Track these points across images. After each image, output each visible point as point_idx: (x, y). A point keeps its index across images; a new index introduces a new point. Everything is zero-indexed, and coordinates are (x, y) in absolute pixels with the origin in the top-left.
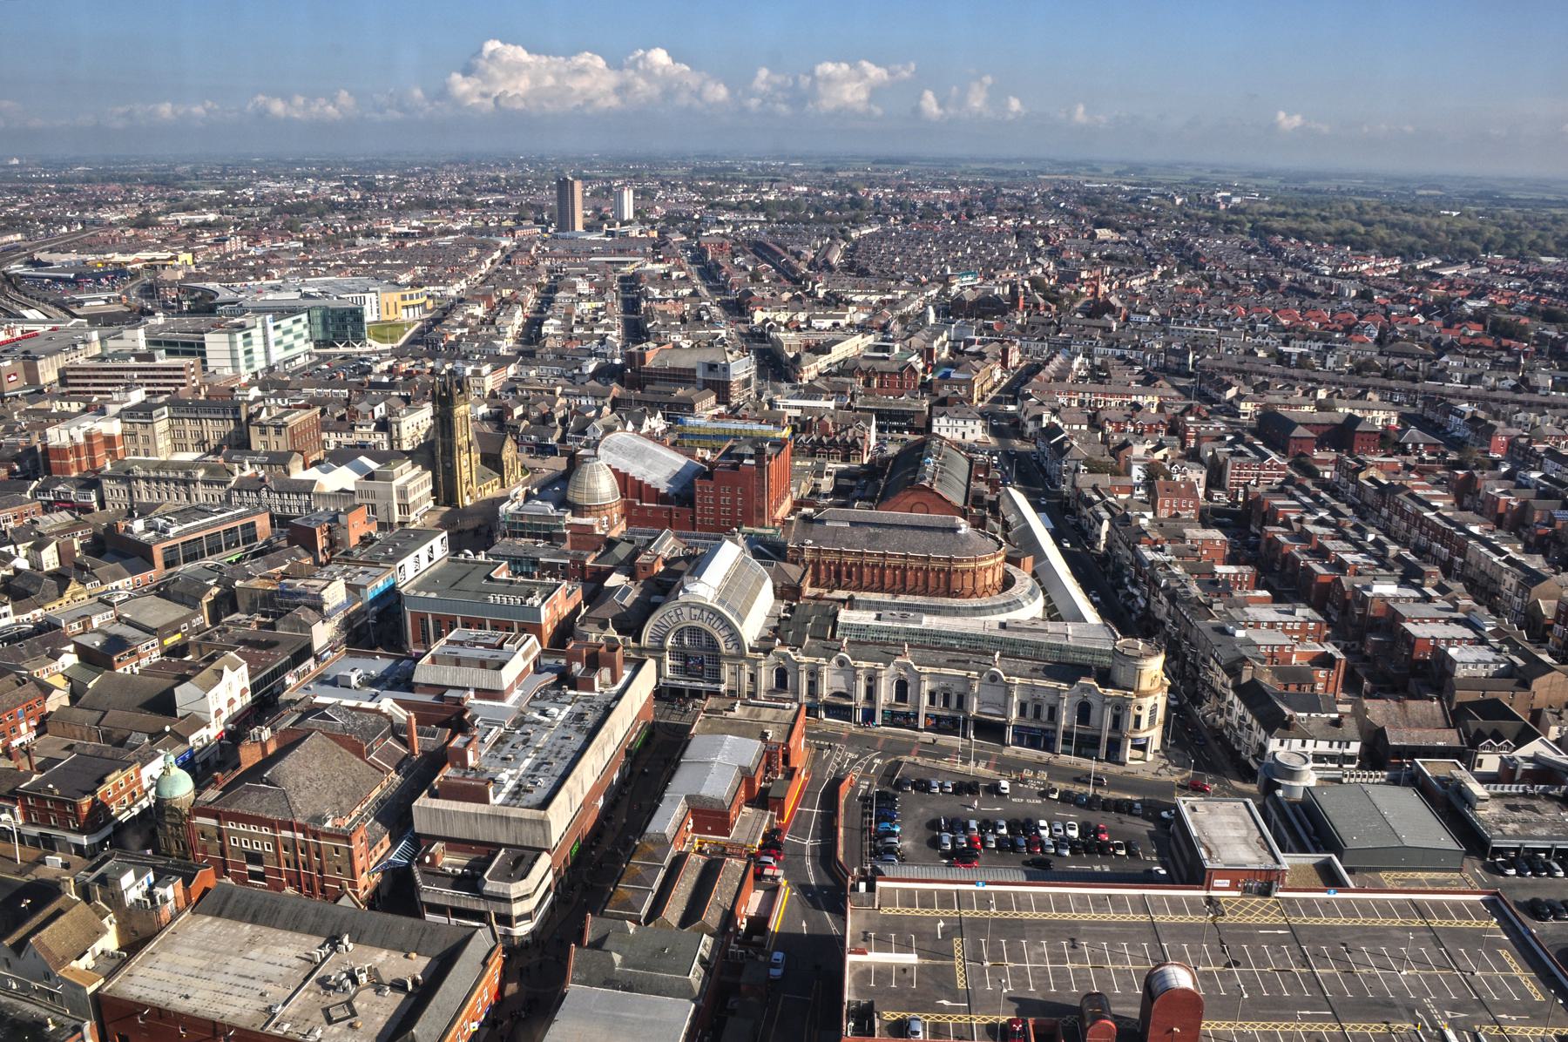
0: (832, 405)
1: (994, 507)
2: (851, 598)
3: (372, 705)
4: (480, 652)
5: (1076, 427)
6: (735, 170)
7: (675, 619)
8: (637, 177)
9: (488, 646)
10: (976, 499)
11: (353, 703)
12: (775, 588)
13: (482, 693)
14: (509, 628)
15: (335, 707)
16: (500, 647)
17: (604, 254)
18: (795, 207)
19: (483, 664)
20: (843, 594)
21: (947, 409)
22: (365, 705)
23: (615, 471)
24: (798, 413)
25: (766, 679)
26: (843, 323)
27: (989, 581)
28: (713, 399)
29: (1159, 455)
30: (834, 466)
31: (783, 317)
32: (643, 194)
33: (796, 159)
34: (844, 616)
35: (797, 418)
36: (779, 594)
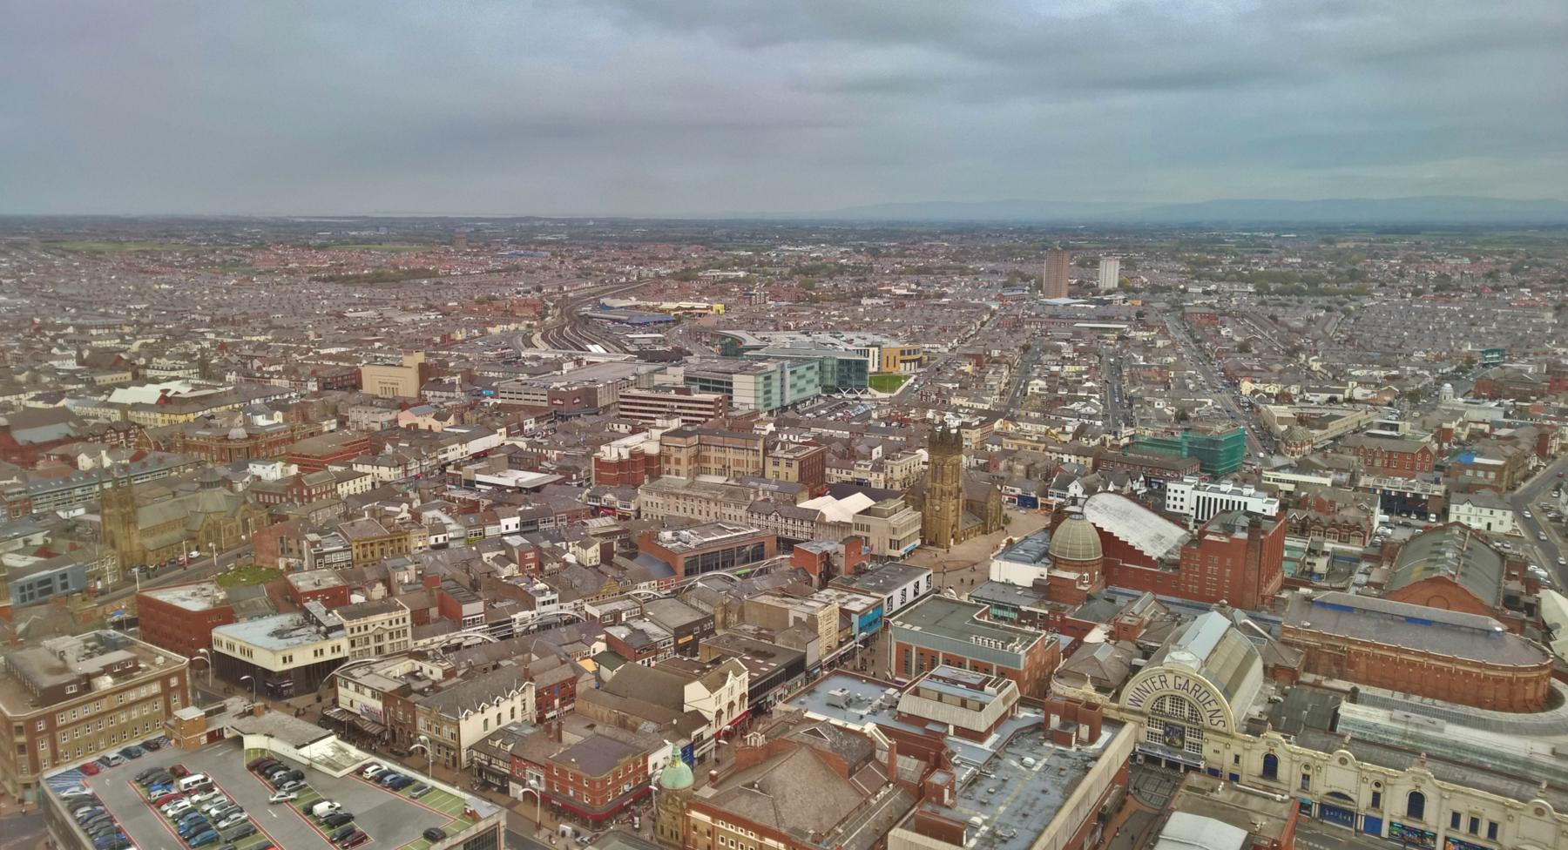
0: (1328, 482)
1: (1532, 609)
2: (1355, 691)
3: (857, 728)
4: (961, 691)
6: (1222, 242)
7: (1158, 685)
8: (1124, 248)
9: (970, 686)
10: (1511, 601)
11: (840, 723)
12: (1265, 668)
13: (962, 732)
14: (987, 670)
15: (825, 724)
16: (982, 689)
17: (1088, 320)
18: (1285, 278)
19: (964, 704)
20: (1345, 685)
21: (1471, 496)
22: (851, 726)
23: (1100, 530)
24: (1291, 487)
25: (1254, 763)
26: (1340, 397)
27: (1530, 695)
28: (1197, 468)
31: (1274, 389)
32: (1129, 264)
33: (1288, 230)
34: (1347, 710)
35: (1288, 493)
36: (1271, 673)
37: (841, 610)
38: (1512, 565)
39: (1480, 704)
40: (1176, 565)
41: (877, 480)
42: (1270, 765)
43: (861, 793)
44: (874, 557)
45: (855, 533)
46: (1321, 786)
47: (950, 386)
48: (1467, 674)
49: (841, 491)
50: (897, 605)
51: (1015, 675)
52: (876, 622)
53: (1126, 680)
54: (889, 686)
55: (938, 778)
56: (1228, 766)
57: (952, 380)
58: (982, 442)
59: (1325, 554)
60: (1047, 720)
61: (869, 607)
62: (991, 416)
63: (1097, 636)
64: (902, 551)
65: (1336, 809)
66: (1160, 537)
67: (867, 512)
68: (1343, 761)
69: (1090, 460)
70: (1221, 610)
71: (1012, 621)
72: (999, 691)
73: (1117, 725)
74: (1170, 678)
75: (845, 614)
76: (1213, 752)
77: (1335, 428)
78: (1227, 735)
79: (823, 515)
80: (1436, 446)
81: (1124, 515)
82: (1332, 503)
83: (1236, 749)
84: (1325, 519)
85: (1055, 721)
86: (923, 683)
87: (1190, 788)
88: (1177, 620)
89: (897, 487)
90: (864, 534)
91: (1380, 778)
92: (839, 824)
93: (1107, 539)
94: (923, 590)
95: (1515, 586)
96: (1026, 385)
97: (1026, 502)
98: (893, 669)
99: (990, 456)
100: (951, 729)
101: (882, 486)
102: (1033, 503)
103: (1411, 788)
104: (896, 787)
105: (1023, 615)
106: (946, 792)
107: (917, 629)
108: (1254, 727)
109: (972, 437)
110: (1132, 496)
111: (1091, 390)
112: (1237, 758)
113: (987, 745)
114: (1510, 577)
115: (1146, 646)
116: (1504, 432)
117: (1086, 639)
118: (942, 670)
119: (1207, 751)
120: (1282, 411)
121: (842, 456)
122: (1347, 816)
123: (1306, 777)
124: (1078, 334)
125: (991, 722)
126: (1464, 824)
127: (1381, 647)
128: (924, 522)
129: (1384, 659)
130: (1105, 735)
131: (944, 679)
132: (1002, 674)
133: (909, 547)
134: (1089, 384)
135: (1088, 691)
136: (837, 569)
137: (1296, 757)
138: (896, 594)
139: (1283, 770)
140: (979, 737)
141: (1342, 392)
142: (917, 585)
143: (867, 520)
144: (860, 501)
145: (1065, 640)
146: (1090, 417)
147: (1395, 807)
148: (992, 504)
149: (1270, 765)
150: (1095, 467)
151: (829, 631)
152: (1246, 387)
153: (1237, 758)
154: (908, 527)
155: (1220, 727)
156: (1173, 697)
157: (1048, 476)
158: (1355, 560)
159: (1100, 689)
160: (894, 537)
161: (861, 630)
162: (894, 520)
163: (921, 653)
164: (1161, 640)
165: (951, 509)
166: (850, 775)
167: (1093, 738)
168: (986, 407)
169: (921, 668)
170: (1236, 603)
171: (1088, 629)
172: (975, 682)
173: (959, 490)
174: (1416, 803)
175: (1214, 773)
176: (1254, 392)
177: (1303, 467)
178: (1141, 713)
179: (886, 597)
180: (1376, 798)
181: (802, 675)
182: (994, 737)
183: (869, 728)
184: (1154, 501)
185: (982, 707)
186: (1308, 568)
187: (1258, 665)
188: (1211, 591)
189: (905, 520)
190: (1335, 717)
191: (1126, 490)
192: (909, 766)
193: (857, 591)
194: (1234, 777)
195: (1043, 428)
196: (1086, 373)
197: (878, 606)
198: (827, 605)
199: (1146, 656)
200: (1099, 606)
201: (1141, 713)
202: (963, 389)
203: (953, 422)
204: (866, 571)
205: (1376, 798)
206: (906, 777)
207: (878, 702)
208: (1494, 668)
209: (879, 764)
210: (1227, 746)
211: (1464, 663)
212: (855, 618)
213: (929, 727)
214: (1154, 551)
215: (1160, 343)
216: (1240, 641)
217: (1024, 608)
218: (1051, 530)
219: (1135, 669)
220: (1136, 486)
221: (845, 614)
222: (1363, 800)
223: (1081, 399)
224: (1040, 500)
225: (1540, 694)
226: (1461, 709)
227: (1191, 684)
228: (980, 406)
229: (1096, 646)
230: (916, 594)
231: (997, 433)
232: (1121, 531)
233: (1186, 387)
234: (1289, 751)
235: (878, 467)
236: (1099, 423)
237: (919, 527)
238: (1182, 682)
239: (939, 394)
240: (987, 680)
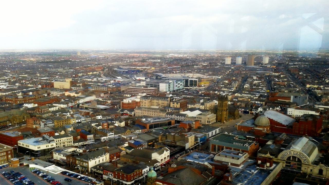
3: (202, 163)
13: (232, 164)
16: (238, 155)
19: (233, 158)
36: (320, 151)
44: (203, 125)
45: (197, 119)
47: (222, 86)
50: (210, 136)
51: (247, 151)
54: (211, 154)
55: (227, 174)
57: (222, 84)
58: (232, 99)
61: (202, 136)
62: (234, 93)
70: (306, 136)
71: (244, 139)
72: (243, 155)
73: (277, 163)
74: (292, 152)
81: (277, 115)
85: (259, 162)
89: (208, 109)
94: (218, 132)
96: (244, 86)
97: (245, 112)
98: (211, 150)
99: (234, 102)
101: (204, 109)
102: (248, 113)
105: (247, 138)
110: (277, 110)
111: (262, 87)
113: (240, 167)
117: (266, 144)
124: (257, 74)
125: (241, 162)
128: (217, 117)
130: (274, 165)
131: (227, 152)
132: (243, 151)
134: (262, 85)
135: (268, 155)
136: (193, 127)
140: (238, 165)
142: (216, 131)
143: (200, 116)
144: (198, 112)
146: (263, 93)
148: (236, 113)
153: (311, 170)
155: (307, 163)
156: (293, 157)
157: (252, 106)
162: (208, 116)
163: (219, 147)
164: (289, 143)
165: (225, 114)
166: (201, 174)
167: (271, 166)
168: (233, 91)
169: (219, 150)
172: (236, 153)
178: (284, 160)
179: (207, 134)
181: (184, 152)
182: (242, 166)
183: (206, 163)
189: (211, 117)
193: (199, 132)
195: (249, 95)
197: (205, 136)
200: (270, 136)
201: (284, 160)
202: (225, 87)
204: (201, 128)
207: (207, 157)
210: (308, 167)
212: (199, 139)
214: (285, 123)
215: (282, 76)
217: (247, 136)
218: (254, 119)
219: (283, 150)
221: (196, 138)
224: (250, 112)
227: (298, 154)
228: (231, 90)
230: (215, 133)
231: (236, 97)
232: (275, 119)
233: (291, 86)
235: (202, 104)
236: (266, 94)
238: (296, 153)
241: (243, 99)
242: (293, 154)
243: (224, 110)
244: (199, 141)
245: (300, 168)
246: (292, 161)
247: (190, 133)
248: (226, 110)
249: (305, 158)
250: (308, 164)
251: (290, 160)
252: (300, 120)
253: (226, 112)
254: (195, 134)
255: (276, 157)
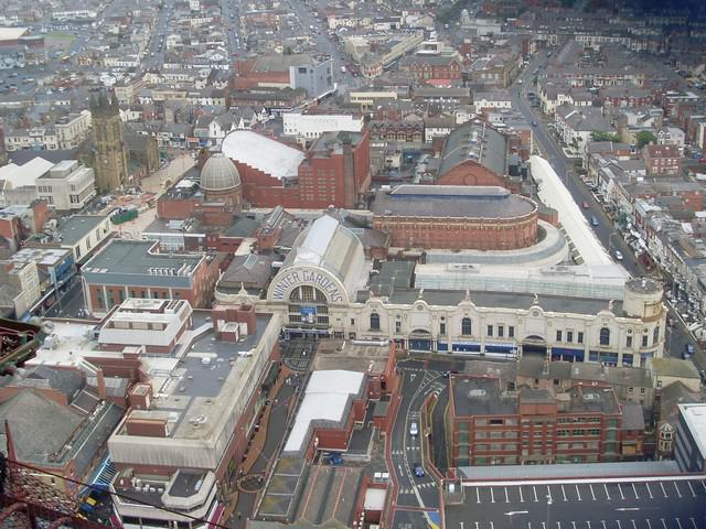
1: (525, 173)
5: (583, 104)
7: (292, 280)
10: (513, 170)
12: (365, 250)
14: (165, 295)
23: (236, 163)
25: (366, 322)
27: (527, 235)
29: (648, 124)
30: (402, 144)
34: (420, 270)
36: (369, 253)
37: (37, 265)
38: (512, 143)
39: (499, 247)
40: (295, 181)
41: (51, 142)
42: (375, 322)
43: (81, 414)
45: (38, 195)
46: (407, 331)
47: (102, 48)
48: (490, 229)
49: (22, 157)
51: (187, 295)
52: (69, 271)
53: (270, 280)
55: (138, 390)
56: (348, 328)
58: (135, 96)
59: (398, 152)
60: (216, 325)
61: (62, 257)
63: (244, 249)
64: (81, 204)
65: (421, 341)
66: (283, 160)
67: (47, 175)
68: (420, 308)
69: (223, 100)
72: (176, 311)
74: (300, 273)
75: (42, 268)
76: (337, 321)
77: (397, 51)
78: (344, 306)
79: (9, 183)
80: (461, 58)
82: (399, 112)
83: (351, 315)
84: (396, 124)
86: (118, 317)
87: (323, 351)
88: (304, 223)
90: (49, 194)
91: (443, 314)
92: (67, 443)
93: (242, 168)
95: (514, 159)
100: (144, 349)
101: (57, 147)
103: (462, 316)
104: (108, 403)
106: (147, 399)
107: (104, 271)
108: (362, 297)
109: (125, 94)
110: (257, 128)
111: (217, 39)
112: (353, 320)
114: (513, 151)
115: (275, 249)
116: (501, 43)
117: (236, 254)
118: (129, 303)
119: (332, 321)
120: (358, 41)
121: (18, 127)
122: (426, 344)
123: (398, 324)
126: (495, 331)
127: (437, 220)
128: (96, 173)
129: (440, 228)
133: (86, 199)
134: (215, 34)
136: (29, 230)
137: (390, 312)
138: (82, 243)
139: (383, 324)
141: (399, 20)
143: (48, 182)
144: (39, 165)
145: (222, 255)
146: (220, 63)
147: (455, 328)
149: (375, 322)
150: (228, 104)
151: (31, 286)
152: (333, 22)
153: (353, 320)
154: (83, 182)
155: (339, 302)
156: (303, 287)
158: (417, 154)
159: (251, 290)
160: (74, 193)
161: (58, 279)
163: (110, 290)
165: (117, 160)
166: (70, 402)
169: (112, 301)
170: (339, 205)
171: (237, 244)
173: (122, 144)
174: (467, 326)
175: (339, 335)
176: (339, 27)
177: (379, 87)
178: (284, 304)
179: (74, 247)
180: (443, 326)
184: (274, 130)
185: (165, 326)
186: (387, 164)
187: (360, 247)
188: (323, 198)
189: (80, 176)
190: (413, 276)
191: (253, 122)
192: (115, 384)
194: (353, 336)
196: (211, 24)
197: (69, 258)
198: (26, 263)
199: (282, 259)
201: (284, 304)
203: (109, 82)
205: (443, 326)
206: (115, 394)
208: (505, 222)
209: (94, 390)
210: (345, 314)
211: (487, 222)
212: (51, 270)
213: (127, 350)
214: (278, 172)
216: (348, 235)
219: (276, 270)
220: (261, 117)
221: (42, 268)
222: (436, 331)
223: (209, 47)
225: (532, 232)
226: (488, 253)
227: (316, 275)
229: (243, 258)
234: (384, 306)
236: (226, 67)
237: (93, 180)
238: (309, 274)
239: (94, 58)
240: (166, 304)
241: (166, 95)
242: (302, 280)
243: (115, 148)
244: (53, 280)
245: (326, 320)
246: (304, 300)
247: (25, 256)
248: (118, 147)
249: (333, 288)
250: (342, 303)
251: (298, 299)
252: (315, 157)
253: (120, 154)
254: (38, 257)
255: (264, 297)
